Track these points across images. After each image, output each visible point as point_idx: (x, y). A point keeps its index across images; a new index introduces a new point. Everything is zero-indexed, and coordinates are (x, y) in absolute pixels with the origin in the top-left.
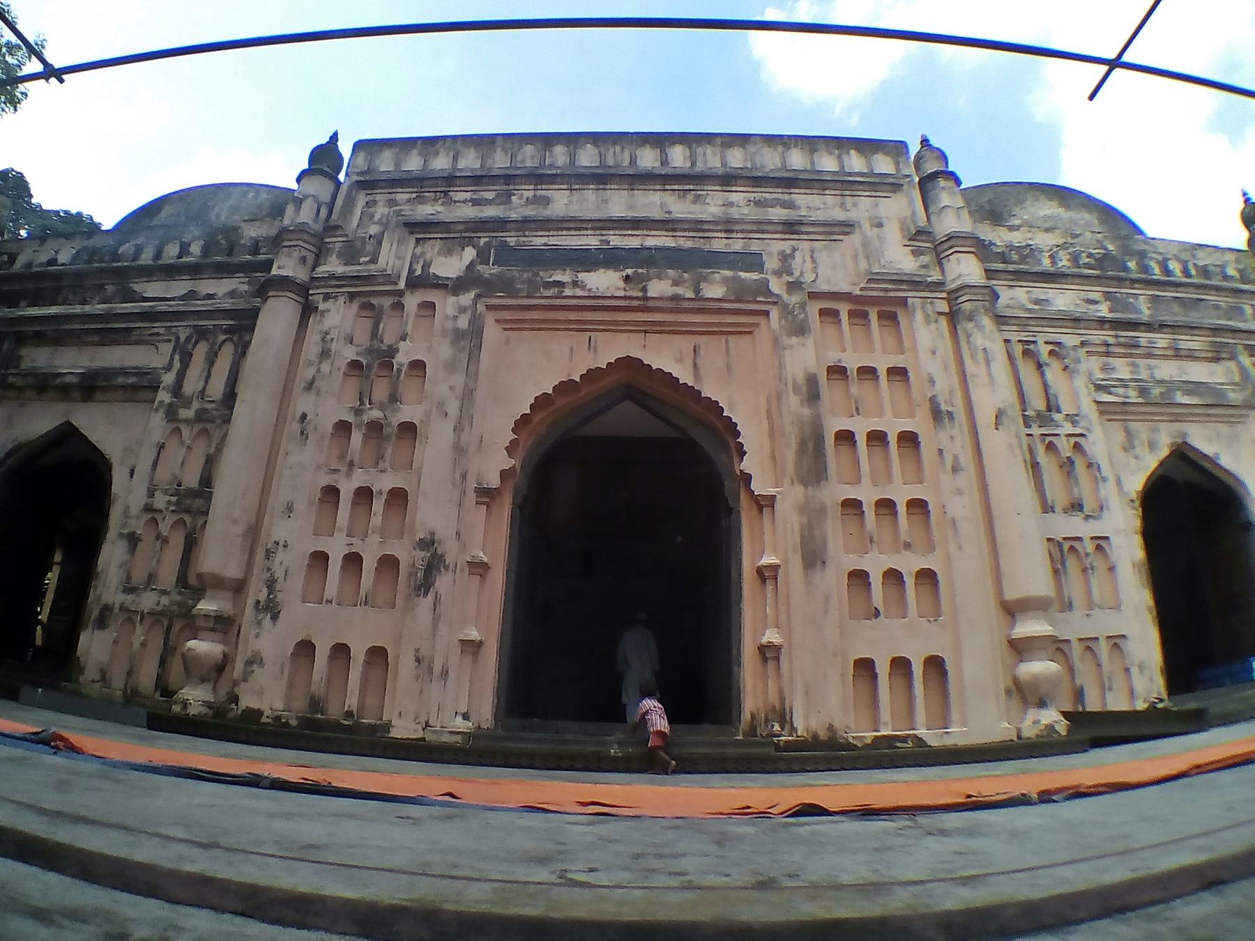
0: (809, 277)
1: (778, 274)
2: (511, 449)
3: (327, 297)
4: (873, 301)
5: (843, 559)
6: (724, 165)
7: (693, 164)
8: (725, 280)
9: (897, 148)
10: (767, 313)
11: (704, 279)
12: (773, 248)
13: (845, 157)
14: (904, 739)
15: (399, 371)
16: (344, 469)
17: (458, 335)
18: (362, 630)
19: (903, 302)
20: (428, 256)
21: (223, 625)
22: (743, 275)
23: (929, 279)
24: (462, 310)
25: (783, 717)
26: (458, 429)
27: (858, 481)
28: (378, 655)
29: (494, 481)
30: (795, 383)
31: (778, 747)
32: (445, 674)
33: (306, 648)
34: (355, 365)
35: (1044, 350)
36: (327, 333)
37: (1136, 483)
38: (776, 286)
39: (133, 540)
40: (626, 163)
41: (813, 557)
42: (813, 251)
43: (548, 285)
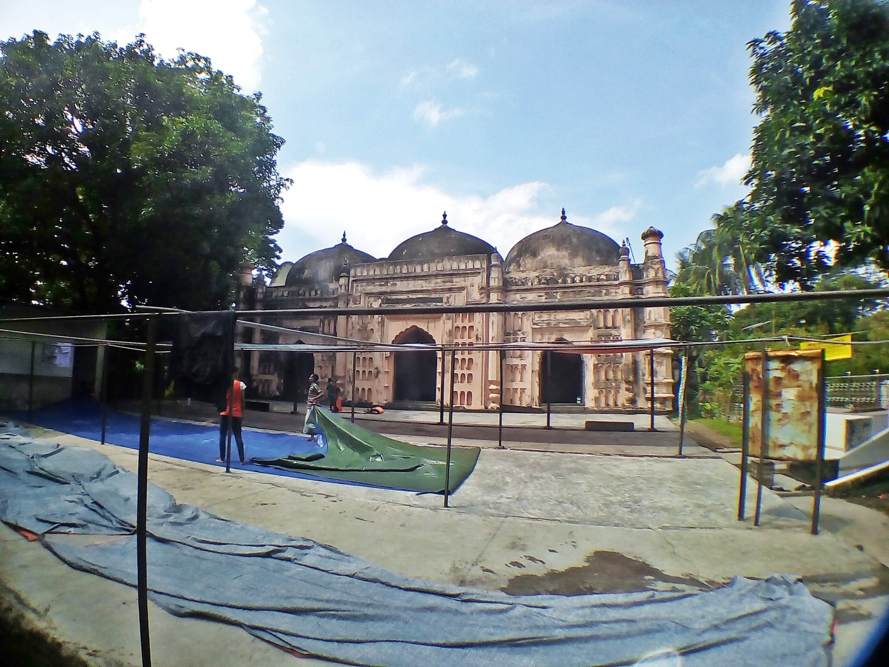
39: (321, 367)
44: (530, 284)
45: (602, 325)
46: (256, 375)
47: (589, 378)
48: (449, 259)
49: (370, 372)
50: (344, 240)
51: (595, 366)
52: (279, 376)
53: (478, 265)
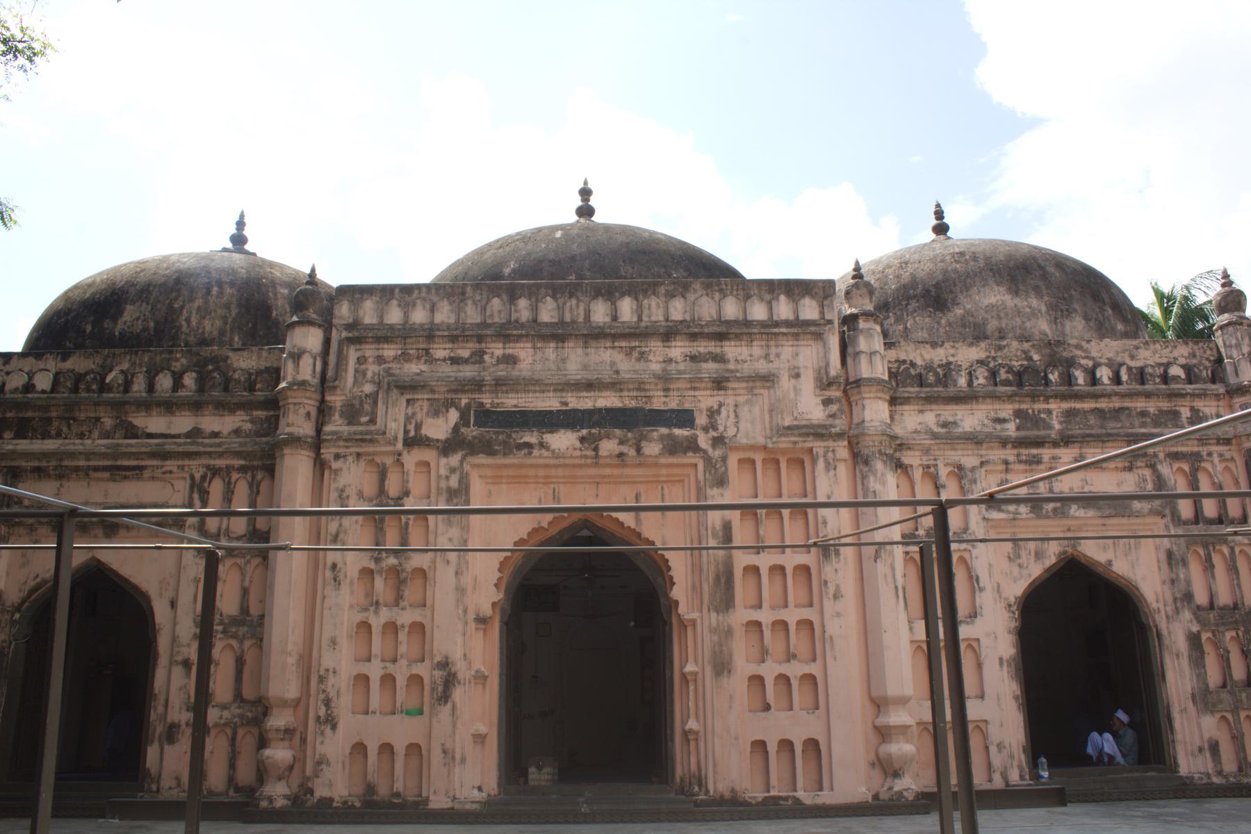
0: (731, 432)
1: (706, 429)
4: (784, 451)
6: (667, 320)
7: (640, 319)
8: (662, 438)
9: (821, 290)
10: (696, 465)
12: (705, 400)
13: (774, 304)
14: (786, 799)
15: (407, 524)
16: (372, 609)
17: (452, 494)
18: (402, 732)
19: (811, 450)
20: (419, 417)
22: (677, 431)
24: (453, 470)
25: (701, 781)
26: (457, 573)
27: (760, 606)
28: (414, 749)
29: (487, 610)
30: (714, 528)
31: (696, 804)
32: (463, 760)
33: (360, 749)
35: (943, 472)
36: (342, 491)
38: (703, 441)
40: (581, 320)
41: (722, 667)
42: (736, 406)
43: (520, 446)
44: (962, 381)
45: (1185, 509)
47: (1177, 681)
48: (708, 287)
49: (416, 680)
51: (1194, 640)
53: (809, 310)
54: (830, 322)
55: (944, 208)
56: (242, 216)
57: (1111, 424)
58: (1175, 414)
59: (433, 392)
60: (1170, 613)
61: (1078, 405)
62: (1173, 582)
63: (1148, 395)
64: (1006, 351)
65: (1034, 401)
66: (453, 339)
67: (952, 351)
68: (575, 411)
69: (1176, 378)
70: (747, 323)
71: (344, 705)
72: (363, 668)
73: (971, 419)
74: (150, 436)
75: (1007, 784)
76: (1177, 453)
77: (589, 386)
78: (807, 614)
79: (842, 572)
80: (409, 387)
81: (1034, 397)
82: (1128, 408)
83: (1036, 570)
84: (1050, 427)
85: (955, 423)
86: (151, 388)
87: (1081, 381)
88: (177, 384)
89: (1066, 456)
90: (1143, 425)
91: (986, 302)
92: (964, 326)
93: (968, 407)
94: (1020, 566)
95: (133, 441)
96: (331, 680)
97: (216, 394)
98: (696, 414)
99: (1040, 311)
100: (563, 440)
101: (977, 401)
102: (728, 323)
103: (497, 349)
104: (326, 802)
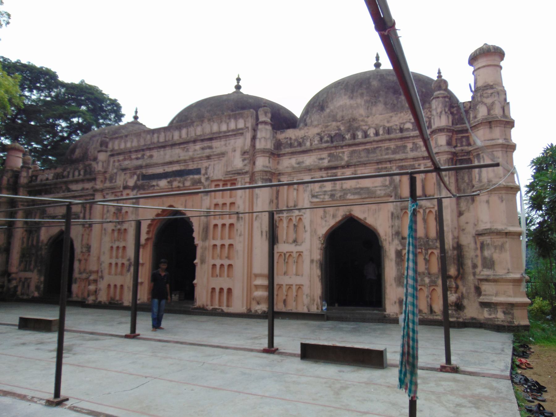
0: (211, 175)
1: (204, 175)
2: (148, 233)
3: (107, 194)
5: (212, 262)
11: (186, 180)
12: (205, 164)
14: (219, 309)
21: (95, 281)
23: (244, 171)
33: (109, 286)
34: (114, 213)
37: (323, 230)
38: (203, 180)
40: (171, 139)
41: (203, 261)
42: (214, 165)
44: (308, 144)
46: (16, 273)
49: (123, 264)
50: (136, 118)
51: (399, 254)
52: (40, 272)
53: (241, 124)
54: (248, 128)
55: (380, 55)
56: (137, 109)
57: (371, 155)
58: (405, 147)
59: (130, 170)
60: (390, 241)
61: (357, 148)
62: (392, 226)
63: (390, 140)
64: (329, 128)
65: (336, 149)
66: (136, 151)
67: (307, 131)
68: (167, 172)
69: (408, 130)
70: (220, 132)
71: (106, 272)
72: (111, 261)
73: (309, 160)
74: (73, 191)
75: (309, 311)
76: (402, 166)
77: (171, 163)
78: (231, 242)
79: (241, 227)
80: (124, 170)
81: (336, 147)
82: (380, 147)
83: (332, 222)
84: (342, 159)
85: (303, 162)
86: (73, 176)
87: (360, 137)
88: (79, 174)
89: (348, 173)
90: (387, 154)
91: (338, 104)
92: (329, 117)
93: (309, 154)
94: (326, 221)
95: (69, 193)
96: (103, 265)
97: (88, 176)
98: (202, 169)
99: (361, 105)
100: (163, 183)
101: (312, 152)
102: (214, 133)
103: (148, 153)
104: (100, 302)
